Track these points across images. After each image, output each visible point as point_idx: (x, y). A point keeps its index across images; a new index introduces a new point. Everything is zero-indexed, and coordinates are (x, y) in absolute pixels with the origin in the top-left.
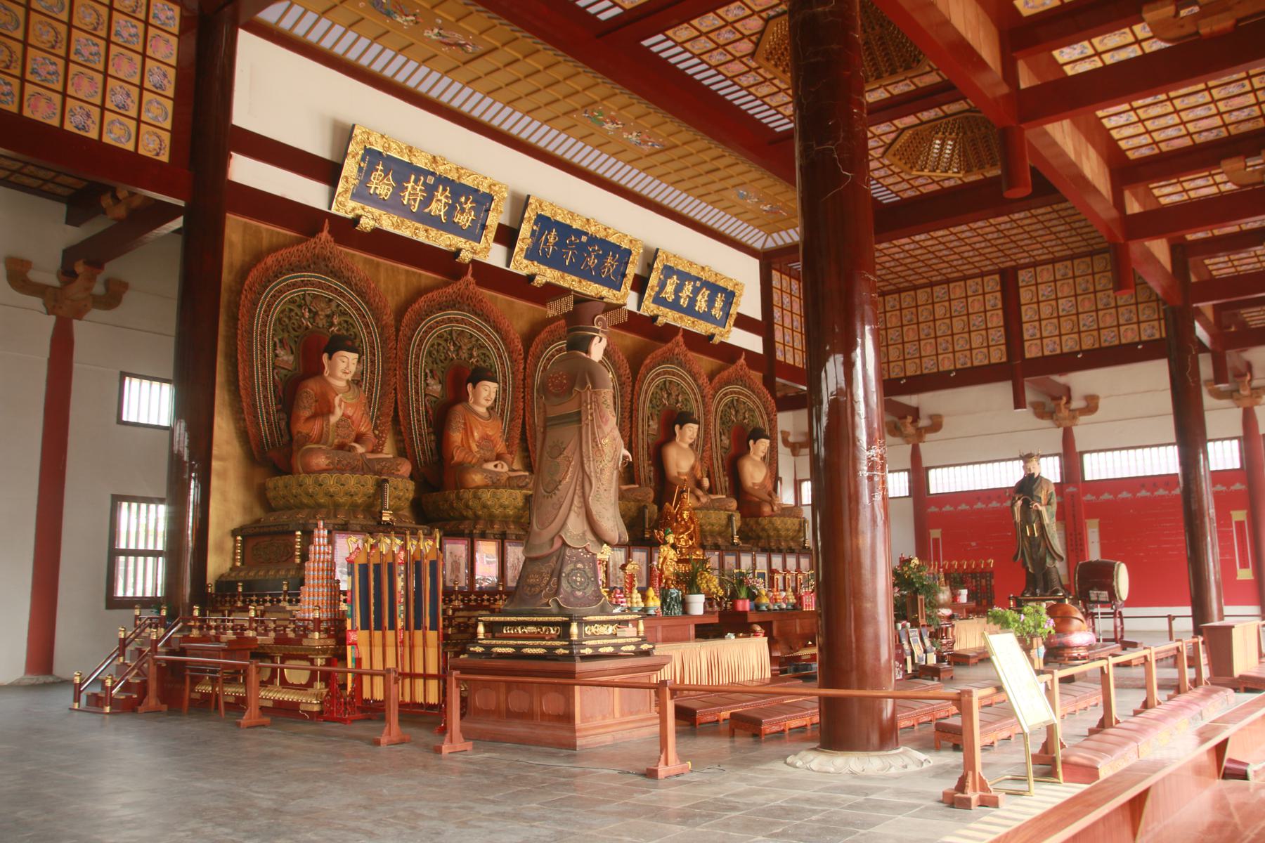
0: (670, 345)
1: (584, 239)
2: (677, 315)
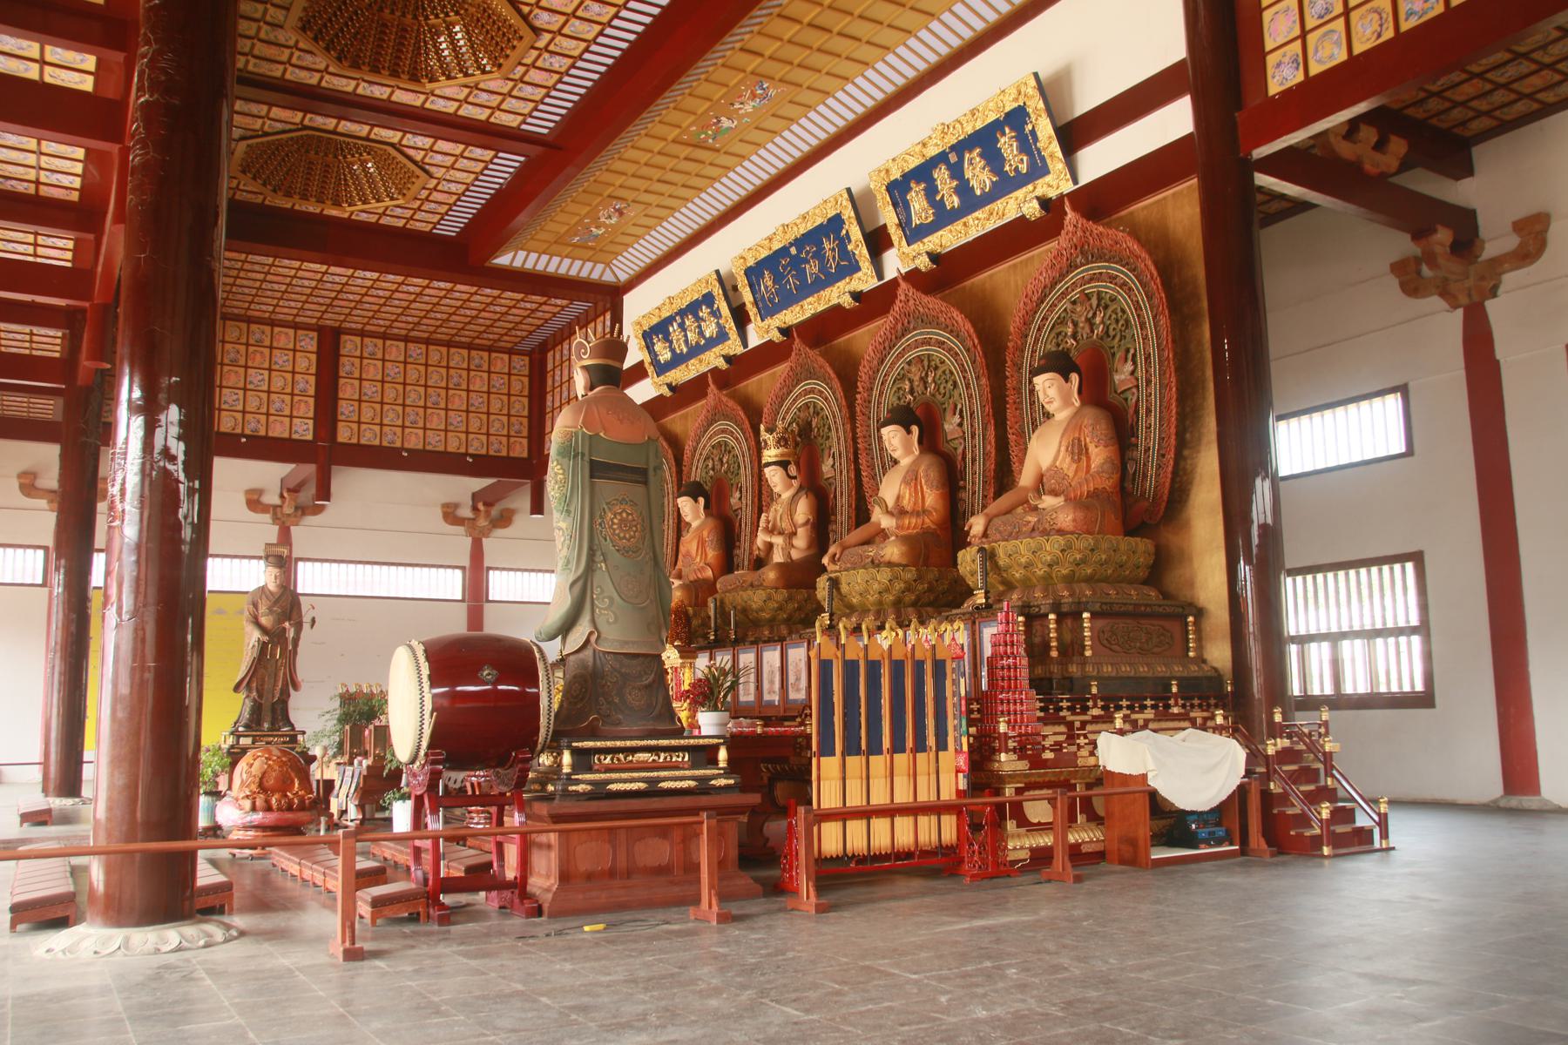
0: (897, 306)
1: (793, 251)
2: (958, 226)
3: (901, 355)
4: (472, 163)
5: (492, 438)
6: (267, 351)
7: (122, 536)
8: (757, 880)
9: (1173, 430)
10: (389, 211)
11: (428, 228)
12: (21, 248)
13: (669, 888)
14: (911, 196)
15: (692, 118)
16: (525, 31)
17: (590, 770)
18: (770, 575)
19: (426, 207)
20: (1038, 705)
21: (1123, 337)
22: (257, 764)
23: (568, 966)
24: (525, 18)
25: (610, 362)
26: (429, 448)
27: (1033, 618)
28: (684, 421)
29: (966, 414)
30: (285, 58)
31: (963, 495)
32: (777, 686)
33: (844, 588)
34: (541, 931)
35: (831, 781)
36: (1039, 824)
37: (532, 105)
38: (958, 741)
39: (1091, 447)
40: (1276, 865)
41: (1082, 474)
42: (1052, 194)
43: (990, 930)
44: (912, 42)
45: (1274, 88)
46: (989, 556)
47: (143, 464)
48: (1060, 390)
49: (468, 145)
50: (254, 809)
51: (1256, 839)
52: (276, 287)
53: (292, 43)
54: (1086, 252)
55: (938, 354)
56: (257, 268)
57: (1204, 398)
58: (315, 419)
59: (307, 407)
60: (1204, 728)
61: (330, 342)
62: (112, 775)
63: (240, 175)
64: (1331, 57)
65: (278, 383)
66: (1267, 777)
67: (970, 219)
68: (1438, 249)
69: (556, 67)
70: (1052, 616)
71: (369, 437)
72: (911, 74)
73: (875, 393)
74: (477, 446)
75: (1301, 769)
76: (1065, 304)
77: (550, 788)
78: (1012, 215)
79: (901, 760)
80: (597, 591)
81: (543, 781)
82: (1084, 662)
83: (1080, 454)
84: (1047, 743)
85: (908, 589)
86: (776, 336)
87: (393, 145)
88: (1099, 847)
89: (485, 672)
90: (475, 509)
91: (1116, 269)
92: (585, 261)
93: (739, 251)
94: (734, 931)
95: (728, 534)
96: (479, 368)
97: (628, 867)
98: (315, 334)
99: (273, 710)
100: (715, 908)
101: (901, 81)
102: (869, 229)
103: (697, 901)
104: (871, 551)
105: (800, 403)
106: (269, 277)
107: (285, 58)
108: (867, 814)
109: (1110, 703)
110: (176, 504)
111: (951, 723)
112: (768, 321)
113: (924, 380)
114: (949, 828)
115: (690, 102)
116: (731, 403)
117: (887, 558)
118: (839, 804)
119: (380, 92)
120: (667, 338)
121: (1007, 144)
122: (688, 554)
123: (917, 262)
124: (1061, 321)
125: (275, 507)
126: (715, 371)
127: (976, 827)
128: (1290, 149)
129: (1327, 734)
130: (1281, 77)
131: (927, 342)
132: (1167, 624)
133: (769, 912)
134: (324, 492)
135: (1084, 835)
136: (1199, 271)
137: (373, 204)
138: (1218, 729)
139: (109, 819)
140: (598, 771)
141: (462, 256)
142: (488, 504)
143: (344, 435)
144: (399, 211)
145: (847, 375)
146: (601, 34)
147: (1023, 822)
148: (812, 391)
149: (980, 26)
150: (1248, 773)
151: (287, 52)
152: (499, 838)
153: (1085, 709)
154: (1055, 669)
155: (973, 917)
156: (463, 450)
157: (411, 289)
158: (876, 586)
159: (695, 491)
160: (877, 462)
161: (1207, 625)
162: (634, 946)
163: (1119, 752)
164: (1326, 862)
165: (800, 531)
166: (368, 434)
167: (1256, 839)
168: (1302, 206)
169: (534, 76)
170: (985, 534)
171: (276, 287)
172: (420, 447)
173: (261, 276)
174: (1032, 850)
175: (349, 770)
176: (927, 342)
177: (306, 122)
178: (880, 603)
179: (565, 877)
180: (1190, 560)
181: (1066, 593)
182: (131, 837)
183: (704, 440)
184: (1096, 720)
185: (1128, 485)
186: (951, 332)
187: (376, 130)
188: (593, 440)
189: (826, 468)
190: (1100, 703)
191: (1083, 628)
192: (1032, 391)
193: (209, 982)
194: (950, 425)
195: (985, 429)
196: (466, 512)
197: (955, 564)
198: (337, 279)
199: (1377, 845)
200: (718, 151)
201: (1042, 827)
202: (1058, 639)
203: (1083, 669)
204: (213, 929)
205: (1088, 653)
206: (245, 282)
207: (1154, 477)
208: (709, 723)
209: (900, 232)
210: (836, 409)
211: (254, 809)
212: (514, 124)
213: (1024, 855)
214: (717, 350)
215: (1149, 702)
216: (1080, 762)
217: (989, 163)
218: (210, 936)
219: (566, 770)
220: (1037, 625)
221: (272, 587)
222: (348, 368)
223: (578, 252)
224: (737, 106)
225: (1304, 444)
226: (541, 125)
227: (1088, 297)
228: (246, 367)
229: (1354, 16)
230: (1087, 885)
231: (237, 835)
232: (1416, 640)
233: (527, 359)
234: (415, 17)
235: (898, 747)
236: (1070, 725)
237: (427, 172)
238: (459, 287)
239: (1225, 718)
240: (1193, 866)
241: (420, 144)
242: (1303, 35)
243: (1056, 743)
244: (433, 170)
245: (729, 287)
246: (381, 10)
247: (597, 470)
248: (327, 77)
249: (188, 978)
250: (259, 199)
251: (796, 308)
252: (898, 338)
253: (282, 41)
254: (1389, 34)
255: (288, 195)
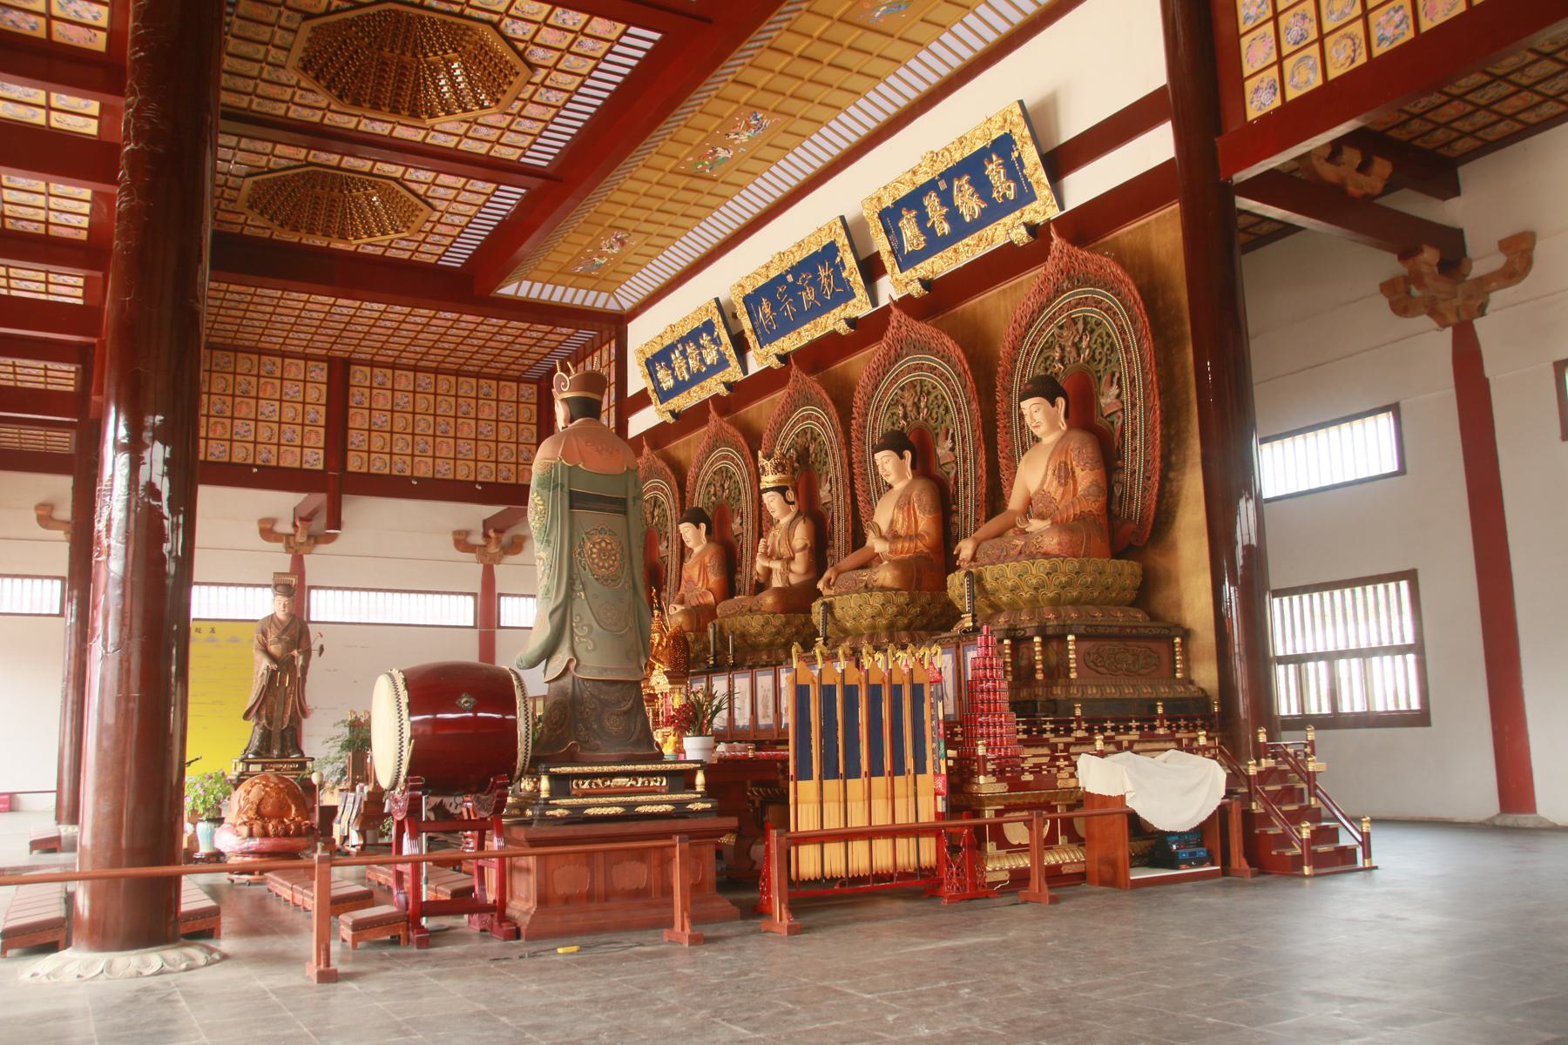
0: (890, 332)
1: (790, 278)
2: (949, 252)
3: (895, 380)
4: (475, 196)
5: (501, 466)
6: (277, 382)
7: (108, 571)
8: (734, 903)
9: (1158, 453)
10: (396, 244)
11: (433, 260)
12: (33, 286)
13: (642, 911)
14: (903, 223)
15: (689, 149)
16: (520, 66)
17: (568, 795)
18: (768, 599)
19: (431, 239)
20: (1021, 727)
21: (1108, 361)
22: (255, 790)
23: (534, 987)
24: (520, 54)
25: (590, 395)
26: (438, 476)
27: (1019, 641)
28: (687, 448)
29: (958, 438)
30: (287, 97)
31: (955, 519)
32: (771, 711)
33: (838, 612)
34: (515, 953)
35: (810, 805)
36: (1020, 845)
37: (530, 138)
38: (936, 764)
39: (1078, 471)
40: (1255, 885)
41: (1069, 497)
42: (1040, 220)
43: (955, 951)
44: (902, 71)
45: (1253, 113)
46: (976, 580)
47: (129, 501)
48: (1047, 414)
49: (469, 178)
50: (251, 835)
51: (1238, 860)
52: (285, 319)
53: (293, 82)
54: (1073, 277)
55: (930, 379)
56: (266, 301)
57: (1188, 421)
58: (326, 449)
59: (318, 437)
60: (1190, 750)
61: (339, 372)
62: (97, 803)
63: (247, 211)
64: (1307, 82)
65: (289, 414)
66: (1249, 797)
67: (960, 245)
68: (1424, 269)
69: (553, 101)
70: (1037, 639)
71: (379, 466)
72: (902, 103)
73: (870, 418)
74: (486, 474)
75: (1284, 788)
76: (1052, 329)
77: (529, 813)
78: (1000, 241)
79: (879, 783)
80: (576, 619)
81: (522, 806)
82: (1069, 683)
83: (1066, 477)
84: (1026, 765)
85: (901, 613)
86: (774, 363)
87: (395, 179)
88: (1080, 868)
89: (464, 700)
90: (486, 535)
91: (1101, 294)
92: (589, 290)
93: (736, 280)
94: (705, 953)
95: (730, 560)
96: (487, 397)
97: (604, 891)
98: (325, 365)
99: (283, 738)
100: (688, 931)
101: (892, 110)
102: (862, 257)
103: (670, 924)
104: (865, 575)
105: (797, 429)
106: (278, 310)
107: (287, 97)
108: (846, 836)
109: (1094, 724)
110: (162, 538)
111: (929, 746)
112: (767, 348)
113: (916, 405)
114: (928, 851)
115: (685, 134)
116: (731, 430)
117: (880, 582)
118: (817, 827)
119: (381, 129)
120: (669, 366)
121: (994, 171)
122: (690, 579)
123: (910, 288)
124: (1049, 346)
125: (288, 536)
126: (716, 397)
127: (954, 849)
128: (1272, 170)
129: (1313, 753)
130: (1259, 102)
131: (919, 368)
132: (1153, 645)
133: (742, 935)
134: (335, 521)
135: (1064, 856)
136: (1183, 296)
137: (379, 238)
138: (1202, 750)
139: (94, 846)
140: (576, 796)
141: (468, 285)
142: (499, 531)
143: (354, 464)
144: (404, 244)
145: (842, 400)
146: (595, 68)
147: (1003, 843)
148: (809, 417)
149: (968, 55)
150: (1229, 793)
151: (290, 91)
152: (481, 862)
153: (1069, 731)
154: (1040, 691)
155: (942, 938)
156: (472, 478)
157: (418, 320)
158: (869, 610)
159: (696, 517)
160: (873, 487)
161: (1194, 646)
162: (603, 967)
163: (1100, 774)
164: (1307, 882)
165: (798, 555)
166: (378, 464)
167: (1238, 860)
168: (1288, 229)
169: (531, 110)
170: (974, 558)
171: (285, 319)
172: (430, 475)
173: (270, 309)
174: (1011, 871)
175: (351, 795)
176: (919, 368)
177: (310, 158)
178: (873, 627)
179: (543, 900)
180: (1177, 581)
181: (1051, 616)
182: (115, 863)
183: (706, 467)
184: (1080, 742)
185: (1115, 508)
186: (942, 358)
187: (379, 165)
188: (572, 471)
189: (824, 493)
190: (1084, 725)
191: (1067, 651)
192: (1021, 416)
193: (183, 1003)
194: (943, 450)
195: (976, 453)
196: (477, 539)
197: (943, 587)
198: (345, 311)
199: (1360, 864)
200: (715, 180)
201: (1021, 849)
202: (1043, 662)
203: (1068, 691)
204: (196, 953)
205: (1073, 675)
206: (255, 315)
207: (1140, 501)
208: (694, 747)
209: (892, 259)
210: (832, 434)
211: (251, 835)
212: (514, 158)
213: (1004, 876)
214: (718, 377)
215: (1134, 724)
216: (1060, 784)
217: (976, 191)
218: (192, 959)
219: (544, 795)
220: (1023, 647)
221: (281, 615)
222: (357, 398)
223: (583, 281)
224: (732, 136)
225: (1286, 466)
226: (541, 158)
227: (1074, 321)
228: (257, 398)
229: (1328, 41)
230: (1063, 906)
231: (234, 860)
232: (1411, 657)
233: (535, 387)
234: (415, 55)
235: (876, 770)
236: (1054, 747)
237: (430, 205)
238: (466, 317)
239: (1208, 738)
240: (1173, 887)
241: (422, 178)
242: (1280, 60)
243: (1036, 766)
244: (436, 203)
245: (728, 314)
246: (381, 48)
247: (577, 500)
248: (329, 115)
249: (166, 1000)
250: (267, 234)
251: (794, 335)
252: (892, 364)
253: (284, 80)
254: (1362, 59)
255: (295, 229)
